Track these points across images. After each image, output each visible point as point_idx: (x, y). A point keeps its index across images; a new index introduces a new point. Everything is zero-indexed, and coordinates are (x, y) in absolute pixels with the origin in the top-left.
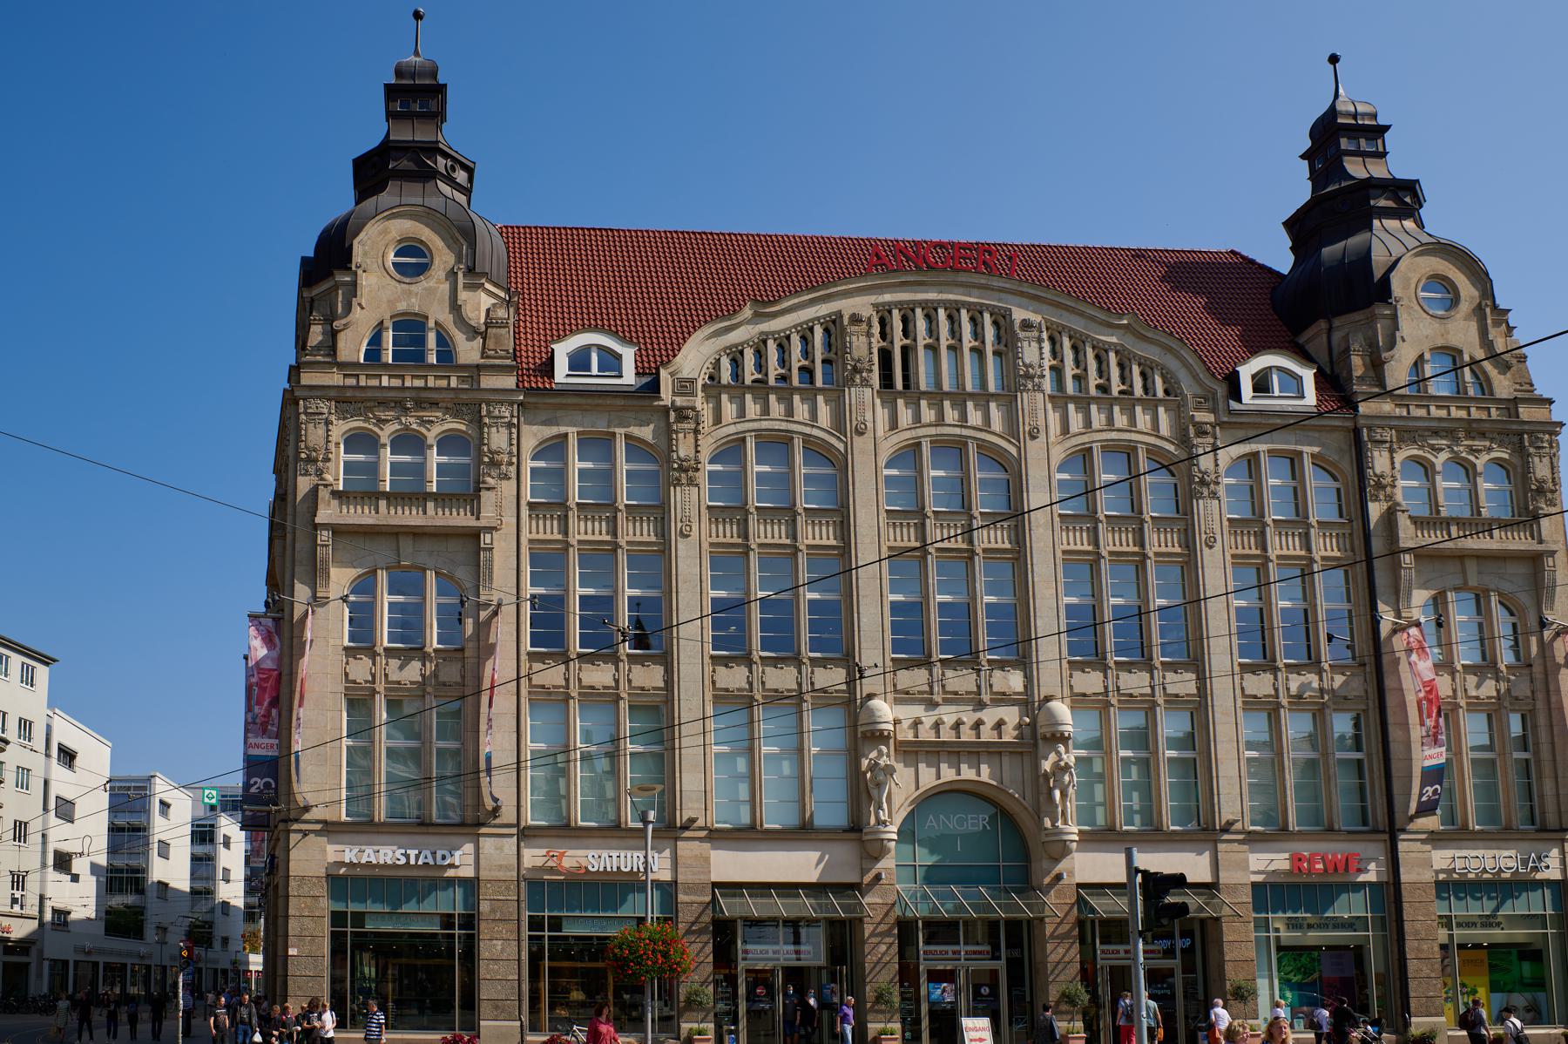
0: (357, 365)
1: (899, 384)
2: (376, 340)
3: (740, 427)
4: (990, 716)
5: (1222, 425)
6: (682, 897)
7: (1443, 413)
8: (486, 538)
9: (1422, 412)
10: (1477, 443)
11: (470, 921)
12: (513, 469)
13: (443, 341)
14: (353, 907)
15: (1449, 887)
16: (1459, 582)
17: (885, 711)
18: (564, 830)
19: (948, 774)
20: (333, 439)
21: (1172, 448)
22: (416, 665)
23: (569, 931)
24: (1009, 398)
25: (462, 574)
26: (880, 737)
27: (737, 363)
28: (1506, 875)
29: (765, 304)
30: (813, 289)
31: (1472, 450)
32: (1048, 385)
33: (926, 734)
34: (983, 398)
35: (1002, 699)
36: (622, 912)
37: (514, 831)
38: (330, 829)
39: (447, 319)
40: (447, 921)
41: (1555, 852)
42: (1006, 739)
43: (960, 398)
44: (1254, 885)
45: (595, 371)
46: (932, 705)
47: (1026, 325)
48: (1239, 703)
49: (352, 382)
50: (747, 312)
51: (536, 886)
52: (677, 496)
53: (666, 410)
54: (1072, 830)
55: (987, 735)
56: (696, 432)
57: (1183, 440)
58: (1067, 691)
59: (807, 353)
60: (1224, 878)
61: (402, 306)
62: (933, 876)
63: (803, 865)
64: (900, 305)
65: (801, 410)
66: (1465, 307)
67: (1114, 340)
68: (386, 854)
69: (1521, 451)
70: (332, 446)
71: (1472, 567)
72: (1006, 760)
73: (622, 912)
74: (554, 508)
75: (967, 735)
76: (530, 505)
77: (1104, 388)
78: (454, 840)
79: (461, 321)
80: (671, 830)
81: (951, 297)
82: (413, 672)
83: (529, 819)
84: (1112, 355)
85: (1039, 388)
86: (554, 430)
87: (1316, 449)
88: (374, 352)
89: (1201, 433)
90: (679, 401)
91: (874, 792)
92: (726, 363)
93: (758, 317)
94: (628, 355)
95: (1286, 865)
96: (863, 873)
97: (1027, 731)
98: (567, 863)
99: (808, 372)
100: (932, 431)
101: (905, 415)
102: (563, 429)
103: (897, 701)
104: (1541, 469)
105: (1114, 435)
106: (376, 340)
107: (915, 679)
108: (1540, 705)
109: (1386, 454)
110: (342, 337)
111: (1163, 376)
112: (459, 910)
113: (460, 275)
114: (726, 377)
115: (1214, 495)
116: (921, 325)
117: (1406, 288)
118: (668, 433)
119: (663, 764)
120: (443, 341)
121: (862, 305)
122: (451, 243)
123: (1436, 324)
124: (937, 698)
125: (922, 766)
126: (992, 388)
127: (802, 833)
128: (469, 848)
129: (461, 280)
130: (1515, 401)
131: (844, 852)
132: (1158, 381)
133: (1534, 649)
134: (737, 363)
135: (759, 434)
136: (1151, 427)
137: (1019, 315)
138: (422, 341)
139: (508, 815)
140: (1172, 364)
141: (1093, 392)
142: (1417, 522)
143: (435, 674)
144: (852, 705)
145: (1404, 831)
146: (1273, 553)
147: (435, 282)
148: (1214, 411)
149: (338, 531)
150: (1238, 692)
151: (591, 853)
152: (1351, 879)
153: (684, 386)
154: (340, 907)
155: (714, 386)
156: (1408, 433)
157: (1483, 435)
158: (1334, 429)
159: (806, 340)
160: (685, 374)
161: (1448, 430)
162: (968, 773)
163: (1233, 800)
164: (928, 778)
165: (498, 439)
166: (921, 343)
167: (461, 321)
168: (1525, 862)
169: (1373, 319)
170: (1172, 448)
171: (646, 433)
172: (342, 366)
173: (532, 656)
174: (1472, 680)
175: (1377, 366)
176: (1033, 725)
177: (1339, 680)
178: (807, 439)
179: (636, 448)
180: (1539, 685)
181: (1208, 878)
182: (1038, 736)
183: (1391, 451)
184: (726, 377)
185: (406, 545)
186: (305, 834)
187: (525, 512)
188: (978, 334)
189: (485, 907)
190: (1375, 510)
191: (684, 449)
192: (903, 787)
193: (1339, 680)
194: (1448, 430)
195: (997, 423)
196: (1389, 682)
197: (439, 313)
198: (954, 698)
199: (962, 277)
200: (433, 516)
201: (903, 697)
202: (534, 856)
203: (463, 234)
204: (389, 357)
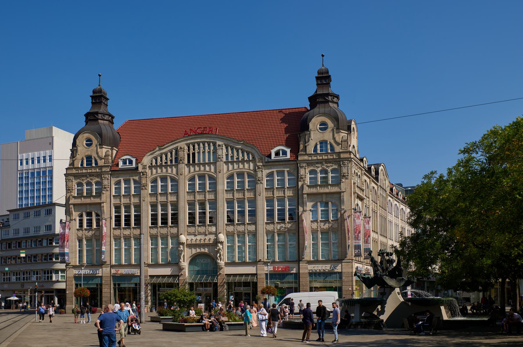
0: (78, 168)
1: (191, 162)
2: (82, 162)
3: (156, 175)
4: (207, 238)
5: (264, 166)
7: (321, 158)
8: (102, 205)
9: (315, 158)
10: (329, 165)
11: (101, 285)
12: (109, 189)
13: (96, 161)
14: (79, 283)
15: (312, 274)
16: (321, 200)
17: (183, 238)
18: (120, 266)
19: (198, 250)
20: (74, 185)
21: (252, 172)
22: (91, 232)
23: (121, 286)
24: (215, 164)
25: (99, 213)
26: (183, 244)
27: (156, 160)
28: (327, 271)
29: (161, 147)
30: (171, 142)
31: (327, 167)
32: (224, 159)
34: (209, 164)
35: (211, 233)
36: (132, 282)
38: (75, 267)
39: (96, 156)
40: (97, 284)
41: (340, 265)
42: (211, 242)
43: (204, 164)
44: (266, 274)
45: (128, 164)
46: (195, 235)
47: (219, 146)
48: (265, 232)
49: (77, 172)
50: (157, 149)
51: (115, 277)
52: (142, 192)
53: (140, 173)
54: (222, 263)
56: (146, 177)
57: (255, 170)
58: (225, 231)
59: (171, 156)
61: (87, 154)
62: (198, 273)
63: (167, 271)
64: (192, 143)
65: (169, 170)
66: (329, 130)
67: (240, 147)
68: (83, 272)
69: (340, 166)
70: (74, 186)
71: (324, 196)
72: (211, 247)
73: (132, 282)
74: (118, 196)
75: (202, 242)
76: (114, 196)
77: (238, 158)
78: (98, 268)
79: (98, 156)
81: (203, 140)
82: (90, 233)
83: (113, 263)
84: (240, 151)
85: (221, 161)
86: (118, 179)
87: (288, 169)
88: (82, 165)
89: (259, 168)
90: (143, 171)
92: (154, 161)
93: (160, 149)
94: (134, 160)
95: (272, 269)
96: (180, 272)
98: (119, 272)
99: (171, 161)
100: (198, 173)
101: (192, 169)
102: (120, 179)
103: (188, 235)
104: (344, 170)
105: (239, 170)
106: (82, 162)
107: (192, 230)
108: (339, 229)
109: (304, 170)
110: (75, 162)
111: (252, 154)
112: (99, 282)
114: (154, 164)
115: (261, 183)
116: (196, 146)
117: (314, 125)
118: (140, 178)
119: (139, 251)
120: (96, 161)
121: (182, 144)
122: (97, 138)
123: (321, 135)
124: (196, 234)
125: (193, 249)
126: (212, 161)
127: (167, 264)
128: (101, 270)
129: (98, 147)
130: (340, 153)
131: (175, 268)
132: (251, 156)
133: (339, 216)
134: (156, 160)
135: (160, 177)
136: (249, 167)
137: (219, 143)
138: (91, 161)
139: (108, 263)
140: (253, 151)
141: (235, 160)
142: (308, 186)
143: (94, 234)
144: (176, 237)
145: (301, 261)
146: (275, 196)
147: (93, 147)
148: (262, 162)
149: (74, 205)
150: (265, 230)
151: (123, 270)
152: (289, 272)
153: (144, 167)
154: (77, 283)
155: (151, 167)
156: (309, 163)
157: (330, 162)
158: (293, 164)
159: (171, 154)
160: (145, 164)
161: (320, 162)
162: (203, 250)
163: (263, 255)
164: (194, 251)
165: (105, 182)
166: (196, 152)
167: (98, 156)
168: (331, 267)
169: (306, 135)
170: (252, 172)
171: (137, 178)
172: (75, 168)
173: (114, 229)
174: (323, 224)
175: (305, 147)
177: (290, 225)
178: (170, 177)
179: (135, 182)
180: (339, 224)
181: (255, 273)
182: (217, 242)
183: (305, 169)
184: (154, 164)
185: (88, 206)
186: (70, 268)
187: (112, 198)
188: (209, 148)
189: (103, 282)
190: (300, 184)
191: (144, 182)
192: (187, 254)
193: (290, 225)
194: (320, 162)
195: (213, 170)
196: (300, 226)
197: (94, 155)
198: (200, 234)
199: (205, 135)
200: (93, 200)
201: (189, 234)
202: (113, 271)
203: (100, 135)
204: (85, 165)
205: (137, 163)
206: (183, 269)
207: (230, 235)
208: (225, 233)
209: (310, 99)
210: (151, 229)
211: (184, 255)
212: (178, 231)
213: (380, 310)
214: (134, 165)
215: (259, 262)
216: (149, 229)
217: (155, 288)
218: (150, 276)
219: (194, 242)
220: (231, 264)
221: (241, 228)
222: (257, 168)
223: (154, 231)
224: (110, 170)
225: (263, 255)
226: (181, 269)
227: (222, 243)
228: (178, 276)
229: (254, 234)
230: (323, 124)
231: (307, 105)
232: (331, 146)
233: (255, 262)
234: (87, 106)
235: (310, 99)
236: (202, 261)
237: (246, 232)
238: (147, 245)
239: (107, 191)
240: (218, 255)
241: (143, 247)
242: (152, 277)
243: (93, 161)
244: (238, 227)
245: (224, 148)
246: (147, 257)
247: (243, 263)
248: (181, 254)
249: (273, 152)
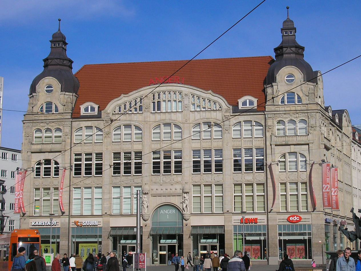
2: (42, 108)
12: (70, 137)
33: (159, 192)
37: (68, 216)
92: (118, 108)
106: (42, 108)
113: (59, 92)
120: (56, 107)
163: (229, 206)
184: (117, 112)
190: (268, 134)
205: (100, 111)
209: (276, 50)
214: (96, 112)
222: (224, 117)
224: (72, 118)
225: (229, 206)
230: (291, 75)
231: (273, 55)
232: (299, 97)
234: (46, 51)
235: (276, 50)
239: (68, 138)
240: (185, 206)
242: (113, 228)
243: (54, 107)
245: (191, 96)
249: (240, 101)
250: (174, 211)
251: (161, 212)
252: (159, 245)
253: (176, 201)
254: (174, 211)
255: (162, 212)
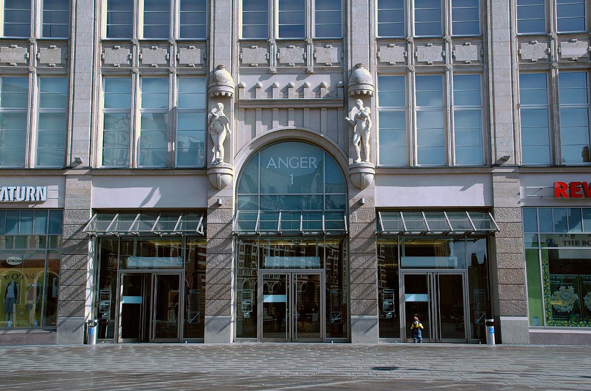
4: (311, 83)
6: (66, 220)
26: (225, 98)
55: (309, 95)
58: (374, 61)
60: (498, 202)
75: (293, 95)
80: (58, 170)
91: (214, 138)
97: (341, 91)
103: (242, 72)
107: (257, 55)
119: (60, 118)
176: (345, 87)
198: (285, 69)
201: (247, 69)
206: (224, 185)
207: (391, 76)
208: (374, 68)
210: (109, 50)
211: (227, 142)
212: (206, 58)
213: (422, 327)
215: (497, 165)
216: (99, 49)
217: (111, 251)
218: (95, 211)
219: (262, 95)
220: (398, 173)
221: (431, 54)
223: (118, 57)
225: (509, 142)
226: (216, 186)
227: (367, 97)
228: (203, 212)
229: (480, 71)
233: (487, 168)
236: (288, 164)
237: (450, 65)
238: (92, 104)
241: (79, 107)
242: (103, 213)
244: (421, 48)
246: (90, 143)
247: (442, 172)
248: (218, 134)
250: (312, 160)
251: (269, 164)
252: (261, 273)
253: (319, 125)
254: (312, 160)
255: (274, 164)
